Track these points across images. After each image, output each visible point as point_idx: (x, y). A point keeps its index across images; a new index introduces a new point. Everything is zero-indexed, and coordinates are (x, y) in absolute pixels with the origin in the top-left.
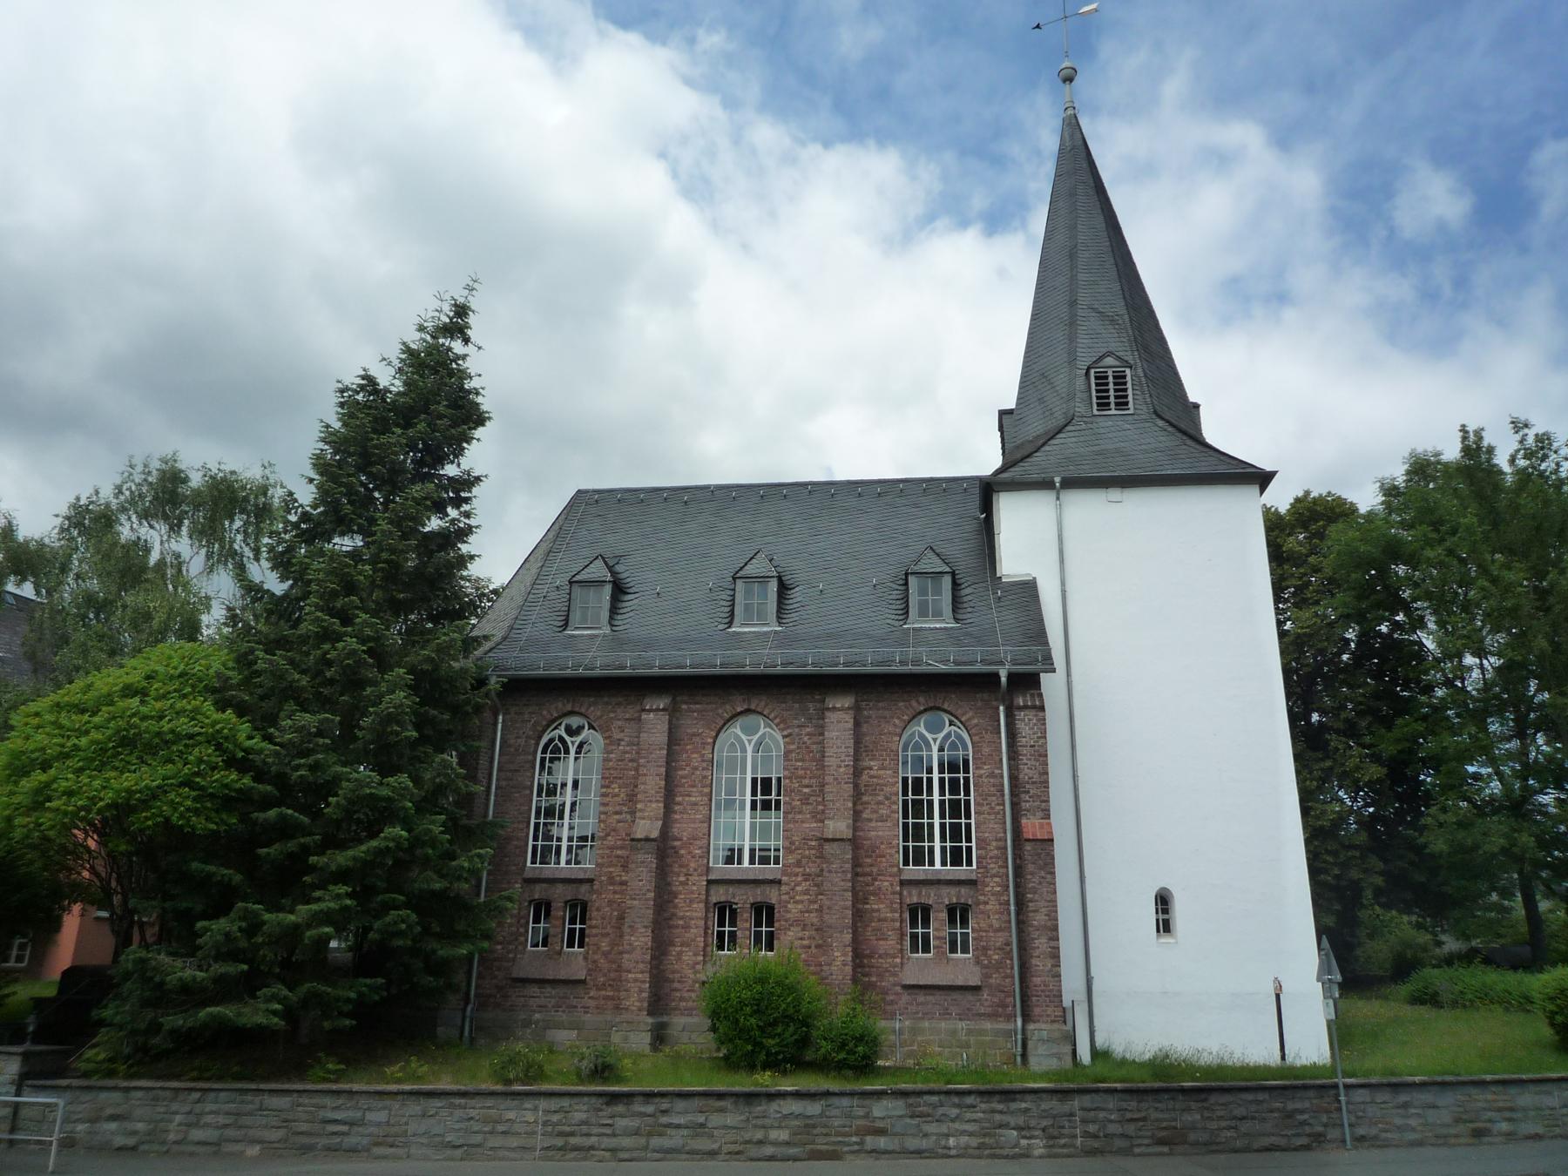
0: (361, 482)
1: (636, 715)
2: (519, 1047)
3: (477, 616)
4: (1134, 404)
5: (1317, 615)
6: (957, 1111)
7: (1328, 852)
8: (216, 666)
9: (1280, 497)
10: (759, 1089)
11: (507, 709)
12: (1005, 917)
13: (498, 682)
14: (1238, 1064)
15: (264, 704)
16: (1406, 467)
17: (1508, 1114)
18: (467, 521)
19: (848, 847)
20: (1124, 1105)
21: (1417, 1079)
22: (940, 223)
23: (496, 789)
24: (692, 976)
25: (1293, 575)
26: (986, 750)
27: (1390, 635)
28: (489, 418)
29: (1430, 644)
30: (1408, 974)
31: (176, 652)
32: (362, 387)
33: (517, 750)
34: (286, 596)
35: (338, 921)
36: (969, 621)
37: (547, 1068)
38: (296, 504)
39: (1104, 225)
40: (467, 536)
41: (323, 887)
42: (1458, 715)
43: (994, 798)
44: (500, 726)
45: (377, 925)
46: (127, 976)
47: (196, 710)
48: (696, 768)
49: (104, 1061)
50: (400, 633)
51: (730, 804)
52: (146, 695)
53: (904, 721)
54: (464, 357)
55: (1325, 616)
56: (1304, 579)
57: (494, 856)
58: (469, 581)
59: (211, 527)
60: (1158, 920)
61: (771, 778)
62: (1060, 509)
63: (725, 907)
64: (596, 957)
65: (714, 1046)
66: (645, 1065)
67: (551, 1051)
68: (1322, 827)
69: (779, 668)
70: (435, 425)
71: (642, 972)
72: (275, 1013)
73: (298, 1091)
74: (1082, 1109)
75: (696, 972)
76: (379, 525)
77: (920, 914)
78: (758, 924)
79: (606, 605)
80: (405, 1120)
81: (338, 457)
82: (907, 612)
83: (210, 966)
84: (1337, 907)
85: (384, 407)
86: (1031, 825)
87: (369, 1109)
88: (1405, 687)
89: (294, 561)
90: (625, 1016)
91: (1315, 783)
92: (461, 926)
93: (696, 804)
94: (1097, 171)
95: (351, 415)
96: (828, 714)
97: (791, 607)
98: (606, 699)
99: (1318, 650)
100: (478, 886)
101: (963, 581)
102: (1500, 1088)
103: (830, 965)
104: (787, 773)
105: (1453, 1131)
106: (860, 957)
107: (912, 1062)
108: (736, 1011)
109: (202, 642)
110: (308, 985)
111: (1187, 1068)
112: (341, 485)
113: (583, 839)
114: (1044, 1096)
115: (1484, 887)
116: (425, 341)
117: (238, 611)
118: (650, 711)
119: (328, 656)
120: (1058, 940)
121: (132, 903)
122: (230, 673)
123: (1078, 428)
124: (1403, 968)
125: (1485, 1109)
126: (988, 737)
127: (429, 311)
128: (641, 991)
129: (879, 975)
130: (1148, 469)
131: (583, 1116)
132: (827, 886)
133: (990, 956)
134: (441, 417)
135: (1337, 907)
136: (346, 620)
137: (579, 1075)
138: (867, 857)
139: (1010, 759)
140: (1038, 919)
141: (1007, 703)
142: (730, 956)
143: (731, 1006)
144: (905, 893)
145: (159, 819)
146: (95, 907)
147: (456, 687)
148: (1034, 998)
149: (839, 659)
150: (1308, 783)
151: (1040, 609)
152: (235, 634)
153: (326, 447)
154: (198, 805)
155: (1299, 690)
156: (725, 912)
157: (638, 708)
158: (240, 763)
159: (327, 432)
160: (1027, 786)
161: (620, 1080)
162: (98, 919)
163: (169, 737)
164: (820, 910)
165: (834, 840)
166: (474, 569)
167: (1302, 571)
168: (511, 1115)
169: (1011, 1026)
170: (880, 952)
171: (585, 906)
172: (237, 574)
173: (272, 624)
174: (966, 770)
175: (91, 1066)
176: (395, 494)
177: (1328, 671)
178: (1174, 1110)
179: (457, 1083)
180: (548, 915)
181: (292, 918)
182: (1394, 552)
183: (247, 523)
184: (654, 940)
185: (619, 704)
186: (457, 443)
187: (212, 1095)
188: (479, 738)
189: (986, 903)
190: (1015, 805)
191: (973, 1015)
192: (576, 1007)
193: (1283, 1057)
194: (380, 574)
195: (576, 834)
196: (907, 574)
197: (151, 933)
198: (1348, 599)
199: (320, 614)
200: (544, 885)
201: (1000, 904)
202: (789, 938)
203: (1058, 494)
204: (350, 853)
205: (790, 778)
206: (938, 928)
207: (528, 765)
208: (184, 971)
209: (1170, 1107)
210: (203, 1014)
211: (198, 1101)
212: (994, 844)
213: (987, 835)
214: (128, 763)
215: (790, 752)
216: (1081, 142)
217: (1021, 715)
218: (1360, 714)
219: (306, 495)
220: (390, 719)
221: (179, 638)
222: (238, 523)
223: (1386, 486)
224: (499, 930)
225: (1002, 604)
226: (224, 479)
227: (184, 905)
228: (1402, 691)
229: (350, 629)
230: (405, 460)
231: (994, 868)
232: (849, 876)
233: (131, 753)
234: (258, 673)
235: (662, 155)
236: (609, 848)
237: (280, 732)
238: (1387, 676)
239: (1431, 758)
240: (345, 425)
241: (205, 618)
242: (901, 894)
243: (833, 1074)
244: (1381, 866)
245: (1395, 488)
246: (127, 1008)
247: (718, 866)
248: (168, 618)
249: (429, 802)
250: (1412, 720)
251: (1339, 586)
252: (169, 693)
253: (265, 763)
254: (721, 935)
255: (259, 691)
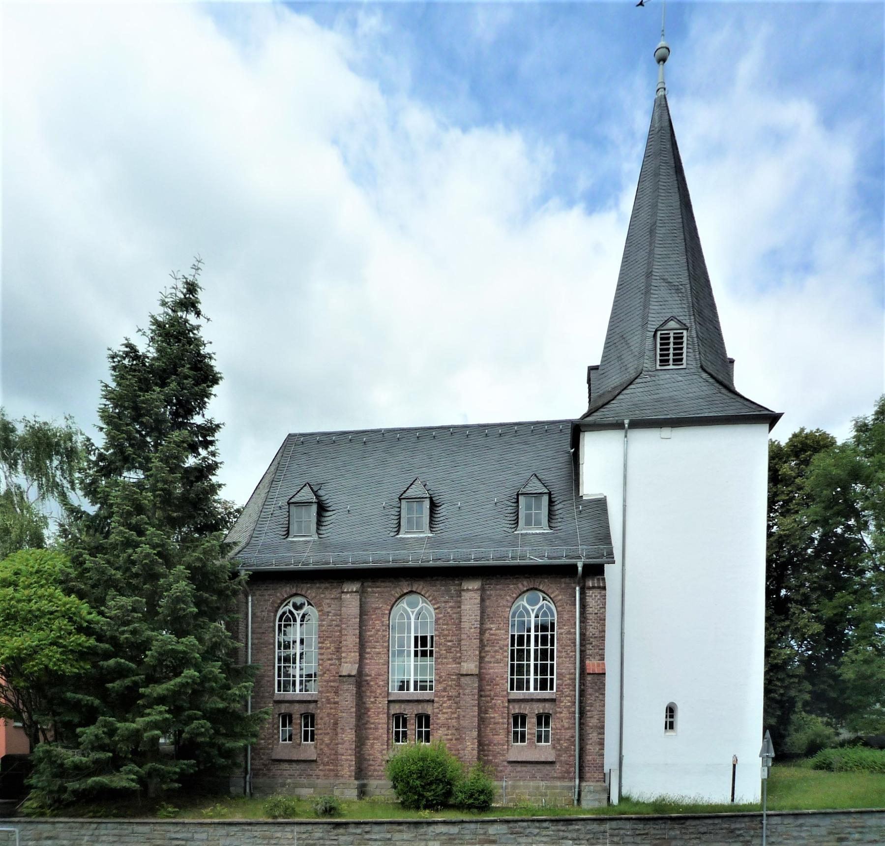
0: (136, 429)
1: (338, 595)
2: (280, 798)
3: (228, 528)
4: (687, 360)
5: (795, 521)
6: (538, 830)
7: (778, 679)
8: (59, 566)
9: (782, 434)
10: (422, 820)
11: (254, 593)
12: (572, 721)
13: (246, 574)
14: (705, 804)
15: (94, 591)
16: (876, 408)
17: (860, 830)
18: (213, 459)
19: (476, 679)
20: (636, 826)
21: (810, 811)
22: (554, 202)
23: (252, 645)
24: (380, 757)
25: (783, 492)
26: (566, 616)
27: (842, 535)
28: (221, 378)
29: (868, 541)
30: (816, 752)
31: (31, 555)
32: (127, 354)
33: (262, 620)
34: (97, 516)
35: (163, 727)
36: (559, 528)
37: (297, 809)
38: (93, 448)
39: (679, 203)
40: (215, 470)
41: (151, 707)
42: (878, 590)
43: (569, 648)
44: (250, 604)
45: (187, 729)
46: (40, 760)
47: (51, 595)
48: (379, 630)
49: (36, 808)
50: (177, 541)
51: (401, 653)
52: (17, 585)
53: (513, 597)
54: (198, 327)
55: (801, 522)
56: (791, 495)
57: (254, 687)
58: (220, 503)
59: (37, 466)
60: (666, 722)
61: (427, 637)
62: (626, 444)
63: (399, 717)
64: (322, 747)
65: (395, 796)
66: (355, 807)
67: (299, 800)
68: (777, 664)
69: (431, 562)
70: (183, 384)
71: (350, 755)
72: (132, 780)
73: (153, 823)
74: (611, 829)
75: (382, 755)
76: (153, 462)
77: (520, 719)
78: (420, 726)
79: (314, 519)
80: (217, 838)
81: (117, 411)
82: (517, 523)
83: (89, 754)
84: (779, 713)
85: (145, 370)
86: (592, 665)
87: (195, 832)
88: (847, 571)
89: (99, 490)
90: (342, 780)
91: (776, 636)
92: (238, 729)
93: (380, 653)
94: (678, 152)
95: (122, 377)
96: (463, 593)
97: (439, 519)
98: (318, 585)
99: (792, 546)
100: (246, 706)
101: (556, 499)
102: (859, 816)
103: (464, 750)
104: (437, 633)
105: (826, 839)
106: (482, 745)
107: (512, 804)
108: (408, 777)
109: (47, 549)
110: (150, 765)
111: (676, 806)
112: (122, 432)
113: (310, 676)
114: (589, 822)
115: (872, 699)
116: (168, 314)
117: (67, 527)
118: (347, 592)
119: (132, 558)
120: (604, 734)
121: (35, 718)
122: (69, 570)
123: (645, 380)
124: (813, 749)
125: (847, 827)
126: (568, 608)
127: (168, 287)
128: (350, 766)
129: (493, 756)
130: (691, 413)
131: (321, 835)
132: (462, 703)
133: (562, 744)
134: (186, 377)
135: (779, 713)
136: (141, 533)
137: (316, 813)
138: (487, 685)
139: (581, 622)
140: (592, 722)
141: (581, 585)
142: (403, 745)
143: (405, 774)
144: (511, 707)
145: (41, 666)
146: (13, 720)
147: (219, 578)
148: (587, 768)
149: (470, 556)
150: (772, 636)
151: (608, 518)
152: (68, 543)
153: (108, 403)
154: (64, 657)
155: (775, 574)
156: (400, 720)
157: (339, 591)
158: (87, 630)
159: (107, 390)
160: (591, 640)
161: (340, 815)
162: (15, 727)
163: (37, 613)
164: (458, 718)
165: (467, 675)
166: (222, 495)
167: (790, 489)
168: (279, 835)
169: (572, 784)
170: (495, 742)
171: (313, 716)
172: (62, 500)
173: (91, 535)
174: (553, 630)
175: (30, 811)
176: (161, 439)
177: (797, 561)
178: (665, 829)
179: (245, 818)
180: (290, 723)
181: (134, 725)
182: (856, 474)
183: (61, 462)
184: (356, 736)
185: (326, 588)
186: (201, 398)
187: (103, 826)
188: (237, 612)
189: (561, 713)
190: (582, 652)
191: (550, 778)
192: (312, 775)
193: (733, 800)
194: (158, 499)
195: (304, 673)
196: (518, 495)
197: (50, 735)
198: (818, 509)
199: (122, 528)
200: (287, 705)
201: (570, 713)
202: (439, 735)
203: (626, 433)
204: (164, 686)
205: (439, 636)
206: (531, 727)
207: (271, 629)
208: (73, 757)
209: (662, 827)
210: (91, 781)
211: (96, 829)
212: (568, 676)
213: (563, 671)
214: (15, 630)
215: (439, 619)
216: (667, 124)
217: (589, 593)
218: (813, 590)
219: (100, 440)
220: (178, 600)
221: (31, 546)
222: (56, 463)
223: (859, 424)
224: (261, 731)
225: (581, 516)
226: (40, 429)
227: (67, 718)
228: (843, 574)
229: (143, 538)
230: (165, 412)
231: (567, 691)
232: (476, 697)
233: (15, 624)
234: (87, 570)
235: (335, 142)
236: (325, 681)
237: (108, 609)
238: (836, 563)
239: (854, 619)
240: (119, 384)
241: (46, 532)
242: (508, 708)
243: (465, 811)
244: (810, 687)
245: (866, 425)
246: (44, 778)
247: (395, 693)
248: (21, 532)
249: (210, 654)
250: (847, 593)
251: (814, 500)
252: (31, 584)
253: (102, 630)
254: (397, 733)
255: (90, 582)
